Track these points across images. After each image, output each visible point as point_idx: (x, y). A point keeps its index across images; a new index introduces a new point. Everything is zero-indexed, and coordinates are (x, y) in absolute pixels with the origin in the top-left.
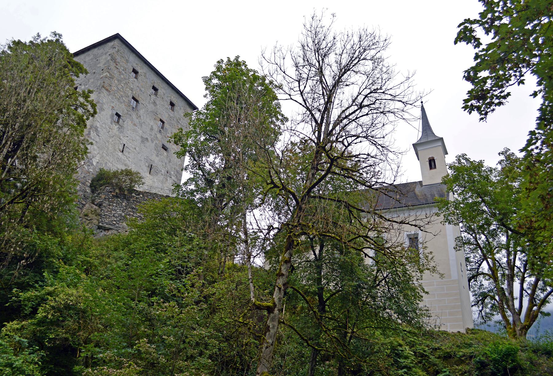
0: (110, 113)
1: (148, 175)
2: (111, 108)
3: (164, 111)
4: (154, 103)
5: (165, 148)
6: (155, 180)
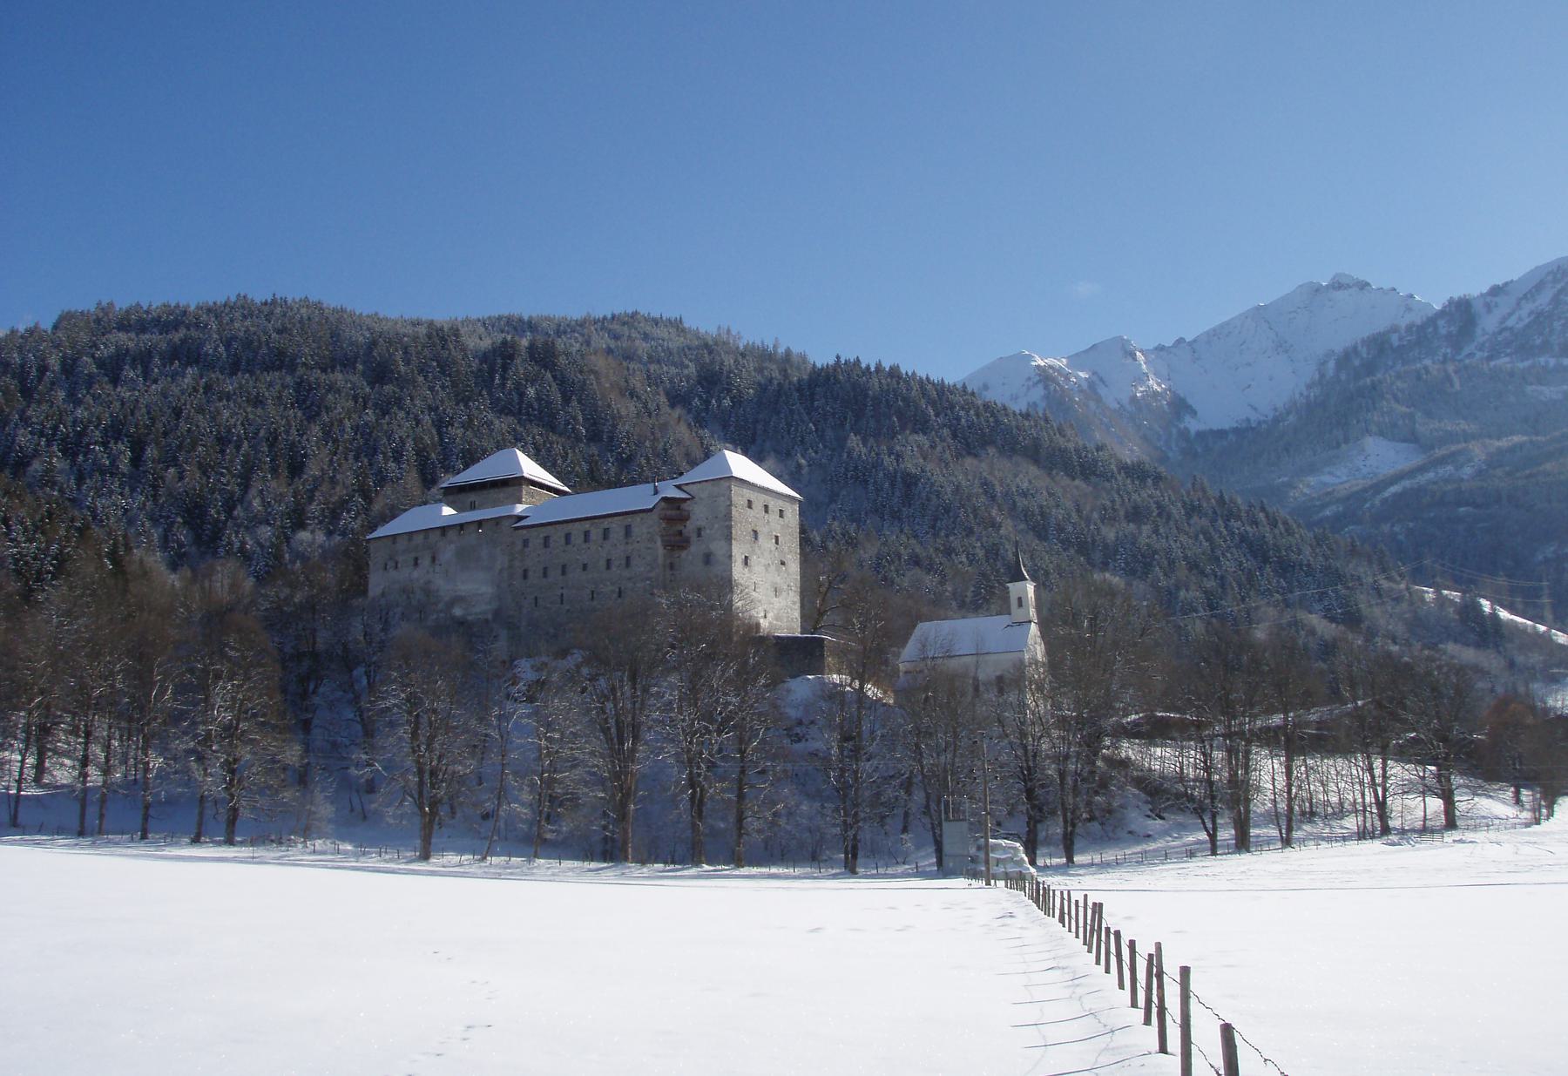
5: (783, 563)
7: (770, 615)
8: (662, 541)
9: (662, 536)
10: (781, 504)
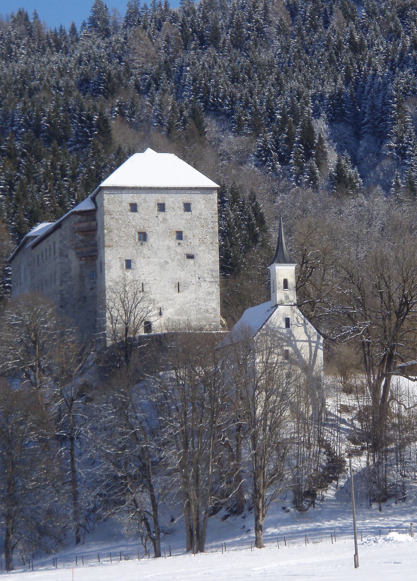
0: (119, 264)
1: (177, 294)
2: (118, 260)
3: (178, 220)
4: (165, 220)
5: (190, 257)
6: (186, 294)
7: (167, 313)
8: (77, 254)
9: (76, 248)
10: (186, 198)
